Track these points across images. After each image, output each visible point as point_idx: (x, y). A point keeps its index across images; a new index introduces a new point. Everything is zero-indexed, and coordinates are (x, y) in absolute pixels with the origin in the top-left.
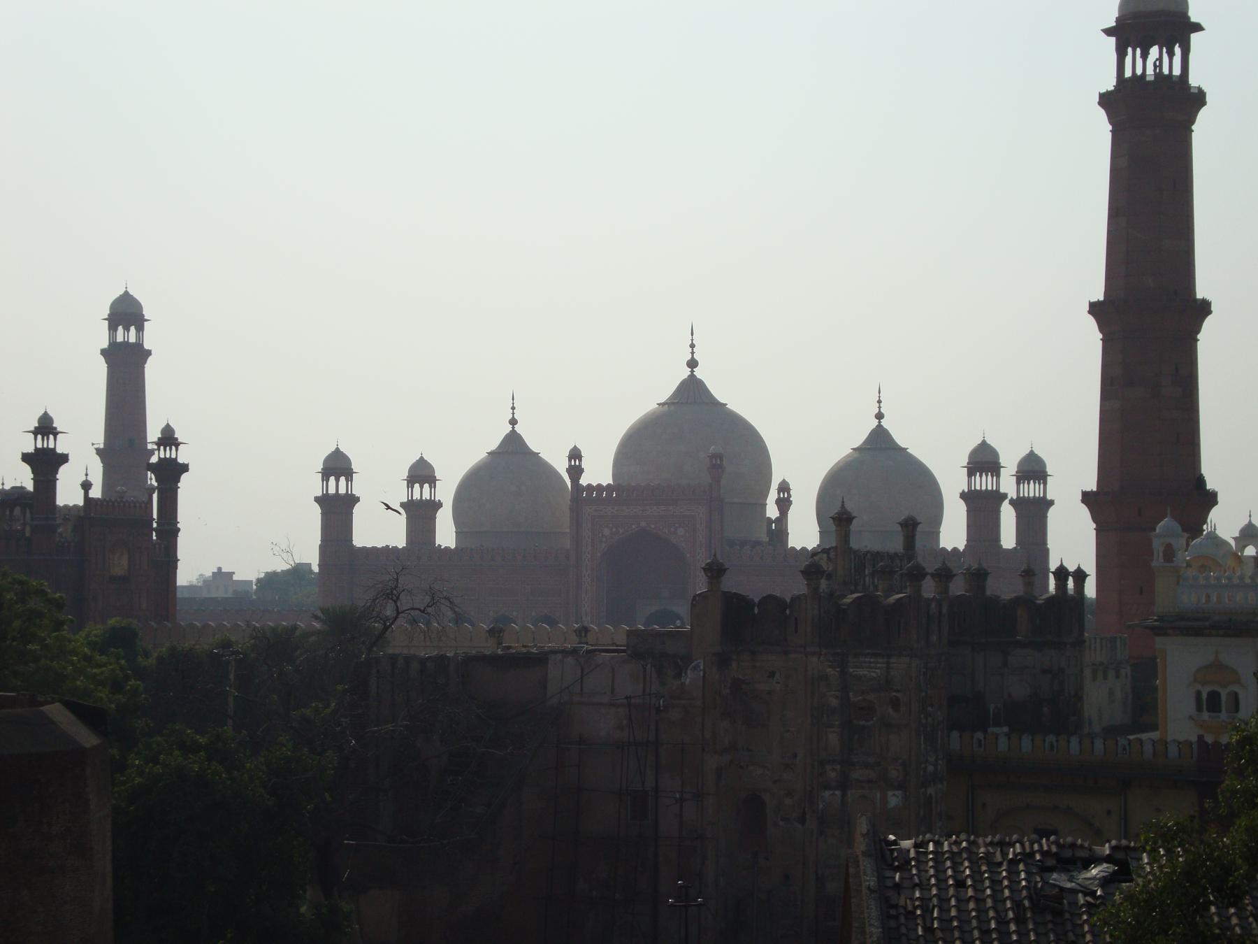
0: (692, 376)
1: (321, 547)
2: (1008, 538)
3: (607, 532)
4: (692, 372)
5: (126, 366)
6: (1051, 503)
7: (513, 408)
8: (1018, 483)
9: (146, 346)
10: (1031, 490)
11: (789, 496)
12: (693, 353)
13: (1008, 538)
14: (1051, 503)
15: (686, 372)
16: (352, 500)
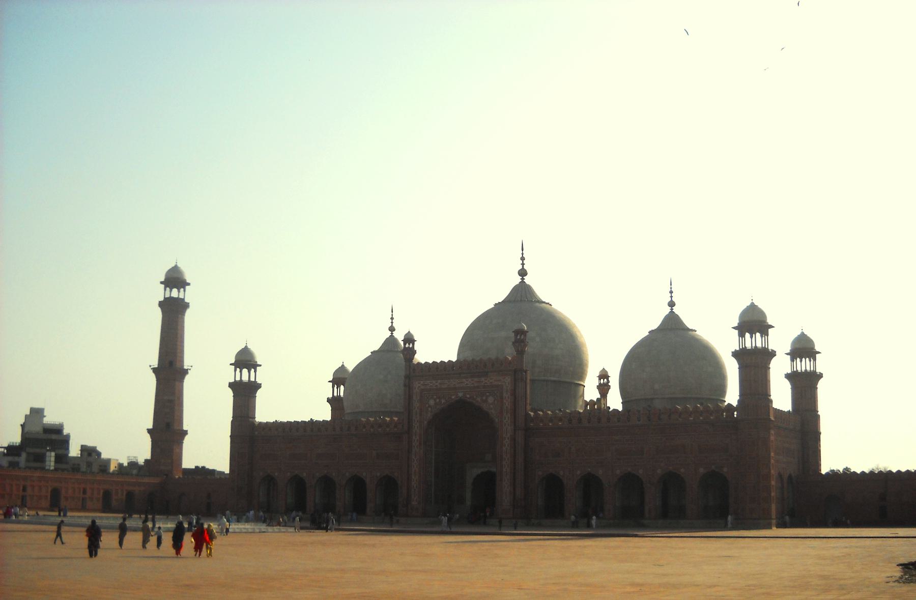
0: (523, 282)
1: (233, 423)
2: (781, 397)
3: (432, 402)
4: (523, 279)
5: (173, 312)
6: (820, 376)
7: (392, 319)
8: (792, 360)
9: (186, 300)
10: (803, 365)
11: (608, 382)
12: (523, 264)
13: (781, 397)
14: (820, 376)
15: (518, 279)
16: (254, 387)
